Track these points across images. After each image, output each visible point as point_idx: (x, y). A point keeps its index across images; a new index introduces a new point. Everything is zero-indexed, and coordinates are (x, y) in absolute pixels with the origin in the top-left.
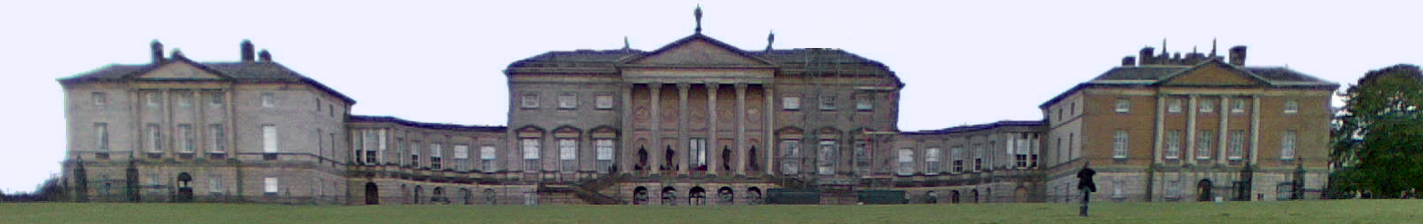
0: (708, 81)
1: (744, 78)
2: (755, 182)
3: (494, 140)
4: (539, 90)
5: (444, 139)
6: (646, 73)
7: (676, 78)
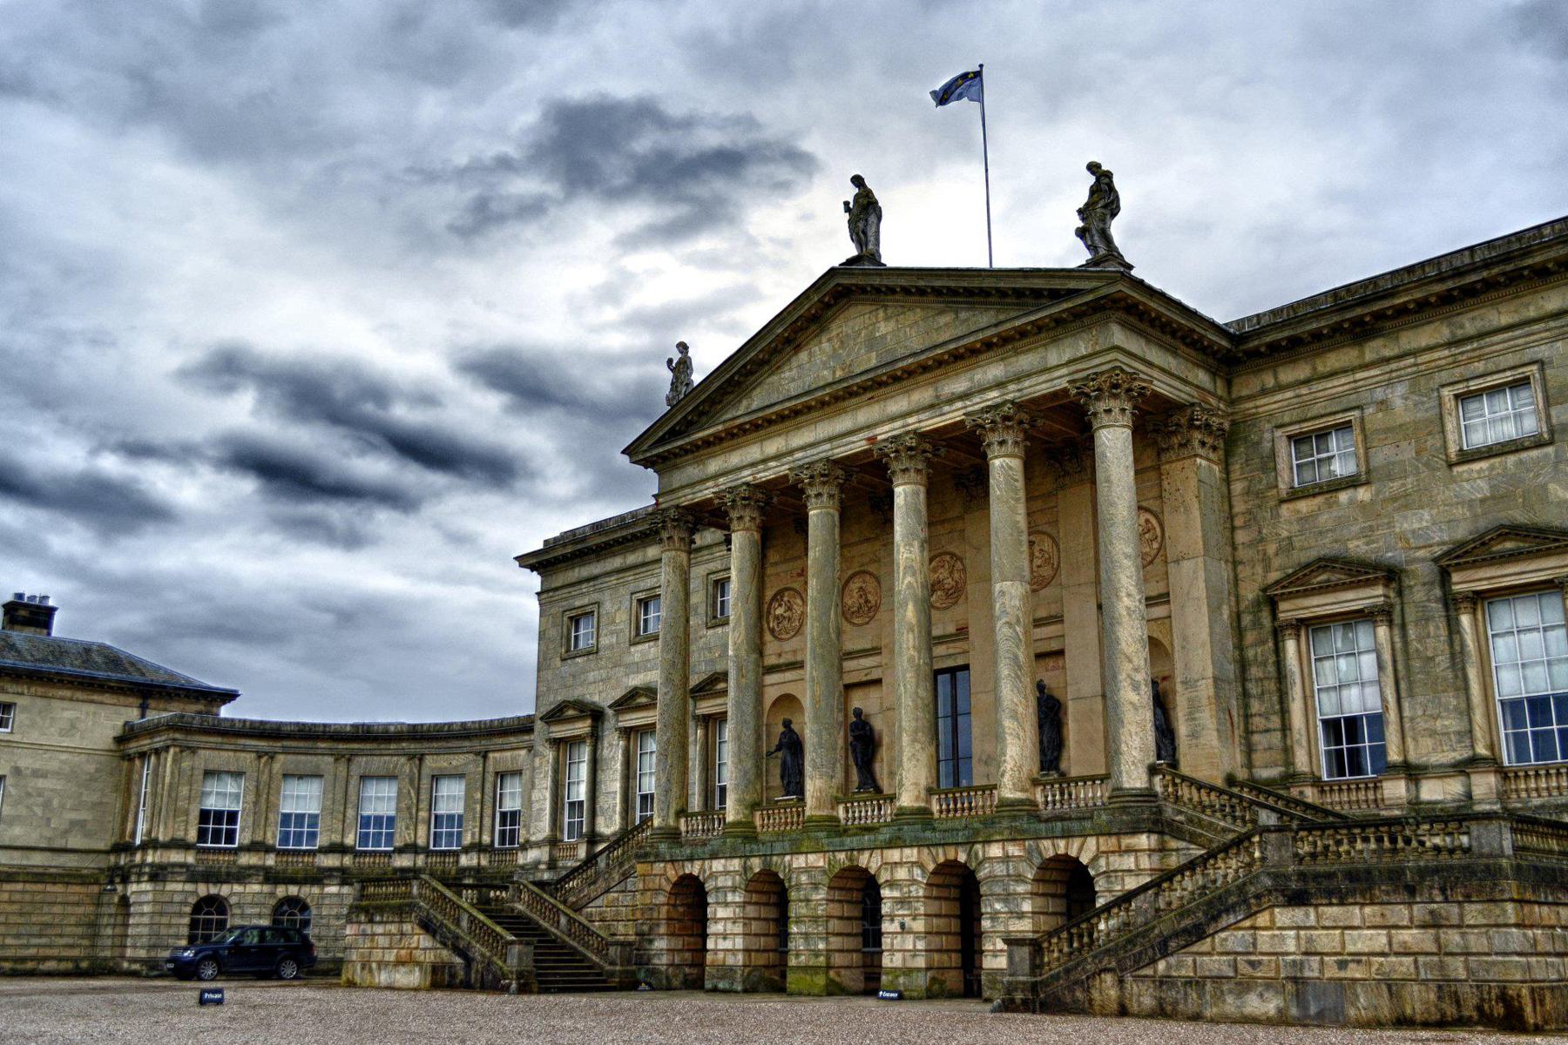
0: (884, 432)
1: (1000, 385)
2: (1067, 835)
3: (458, 761)
4: (595, 597)
5: (404, 765)
6: (714, 466)
7: (791, 452)
